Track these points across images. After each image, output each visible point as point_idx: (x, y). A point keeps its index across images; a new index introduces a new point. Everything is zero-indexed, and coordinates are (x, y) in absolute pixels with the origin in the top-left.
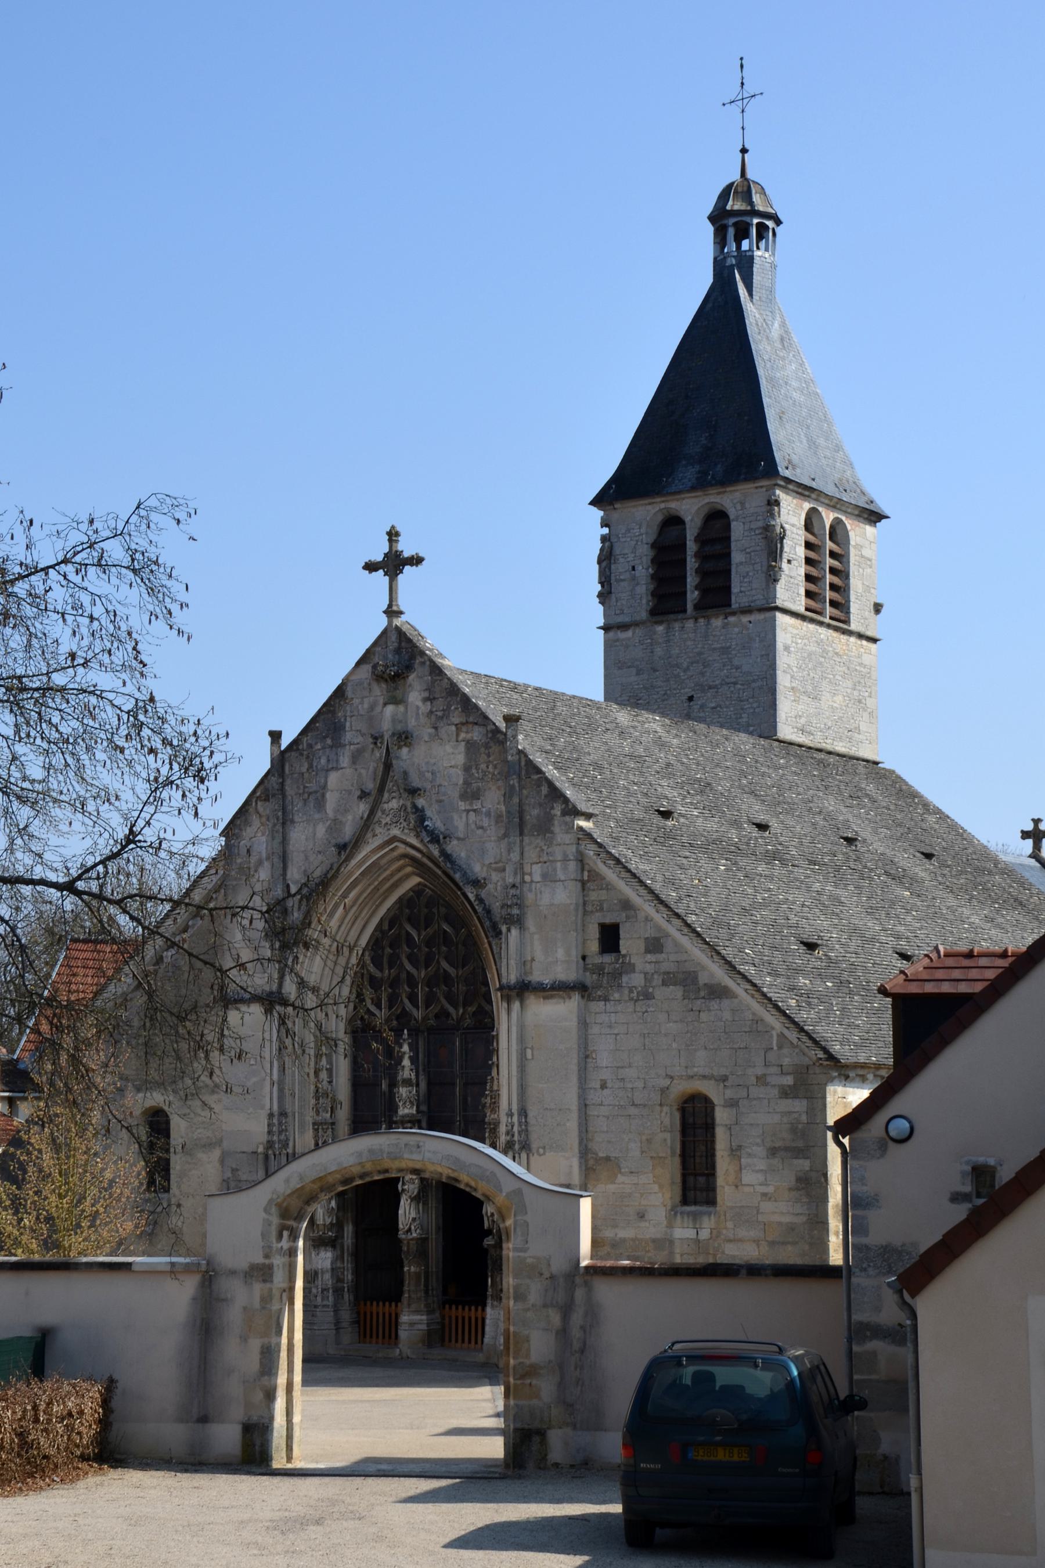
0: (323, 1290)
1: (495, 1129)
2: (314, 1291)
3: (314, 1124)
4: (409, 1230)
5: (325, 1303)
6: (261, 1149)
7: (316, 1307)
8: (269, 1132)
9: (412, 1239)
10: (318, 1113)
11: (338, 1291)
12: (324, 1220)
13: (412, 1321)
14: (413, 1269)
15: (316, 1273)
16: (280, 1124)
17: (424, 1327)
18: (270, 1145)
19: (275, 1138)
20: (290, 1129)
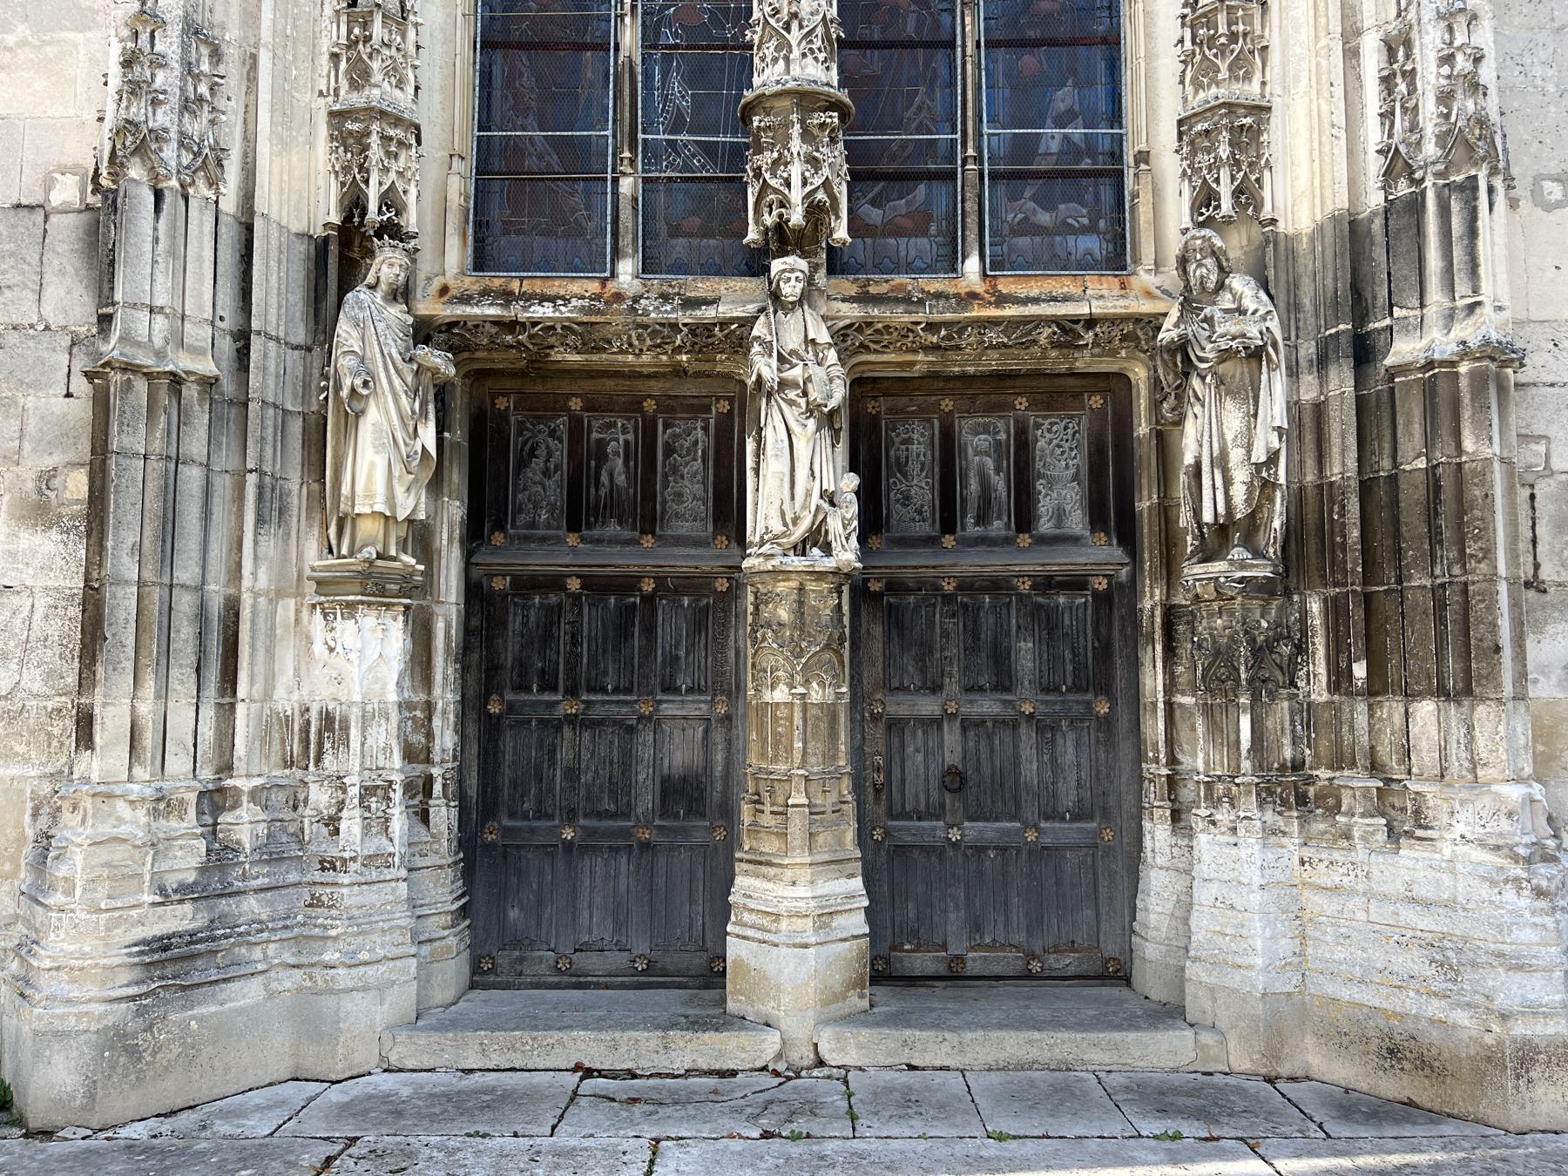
0: (367, 791)
1: (1255, 132)
2: (320, 797)
3: (338, 117)
4: (817, 538)
5: (378, 843)
6: (67, 192)
7: (327, 865)
8: (134, 88)
9: (820, 576)
10: (360, 77)
11: (420, 789)
12: (391, 500)
13: (795, 913)
14: (816, 694)
15: (332, 725)
16: (189, 68)
17: (857, 923)
18: (134, 141)
19: (163, 118)
20: (232, 112)
